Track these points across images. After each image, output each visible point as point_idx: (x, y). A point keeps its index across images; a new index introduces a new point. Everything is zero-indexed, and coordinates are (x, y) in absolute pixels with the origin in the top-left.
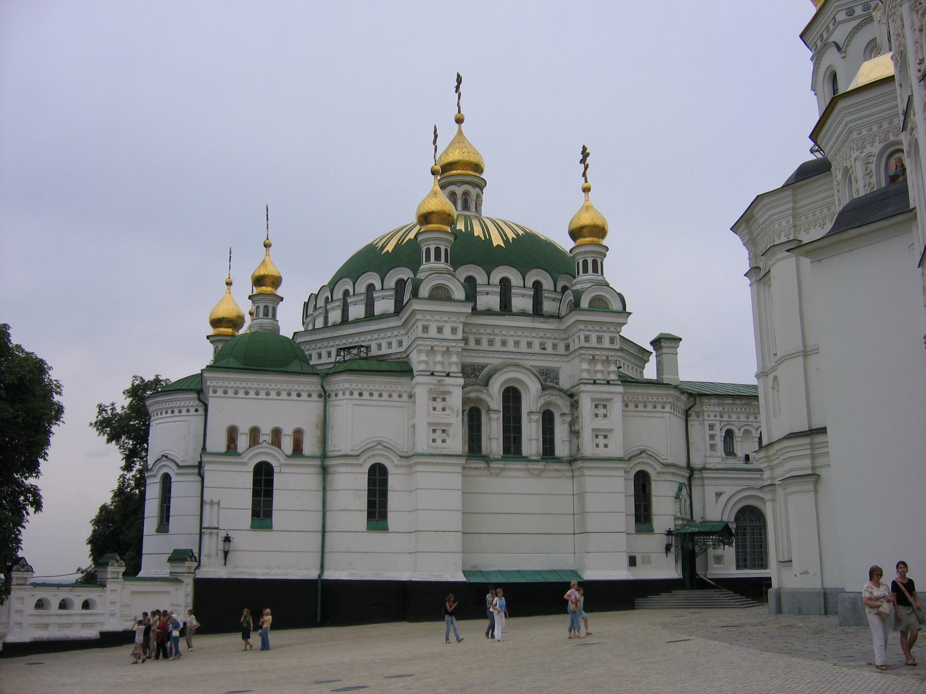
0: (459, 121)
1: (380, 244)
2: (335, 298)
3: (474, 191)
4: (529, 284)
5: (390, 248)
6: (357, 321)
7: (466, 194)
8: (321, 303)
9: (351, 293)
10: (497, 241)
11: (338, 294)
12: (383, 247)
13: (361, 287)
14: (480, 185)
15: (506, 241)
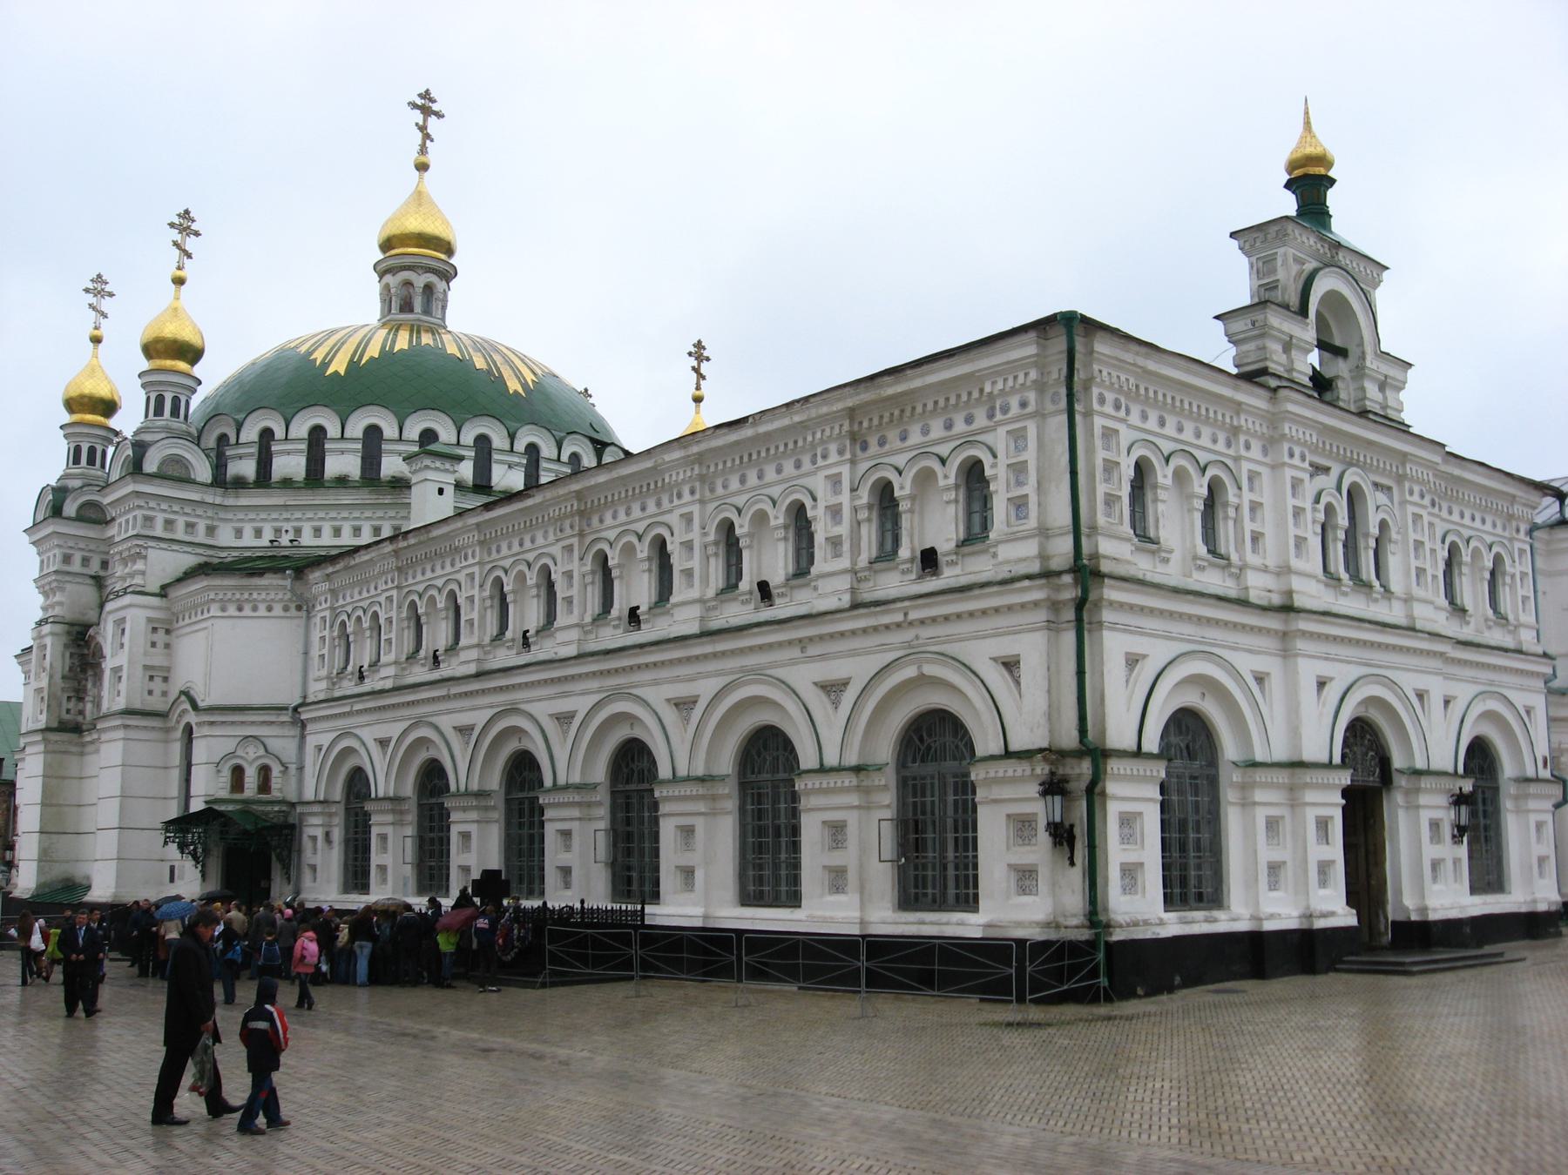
0: (422, 167)
1: (319, 356)
2: (243, 439)
3: (441, 286)
4: (565, 457)
5: (339, 366)
6: (287, 483)
7: (428, 289)
8: (210, 441)
9: (279, 433)
10: (513, 385)
11: (251, 433)
12: (326, 365)
13: (301, 428)
14: (448, 274)
15: (525, 385)
